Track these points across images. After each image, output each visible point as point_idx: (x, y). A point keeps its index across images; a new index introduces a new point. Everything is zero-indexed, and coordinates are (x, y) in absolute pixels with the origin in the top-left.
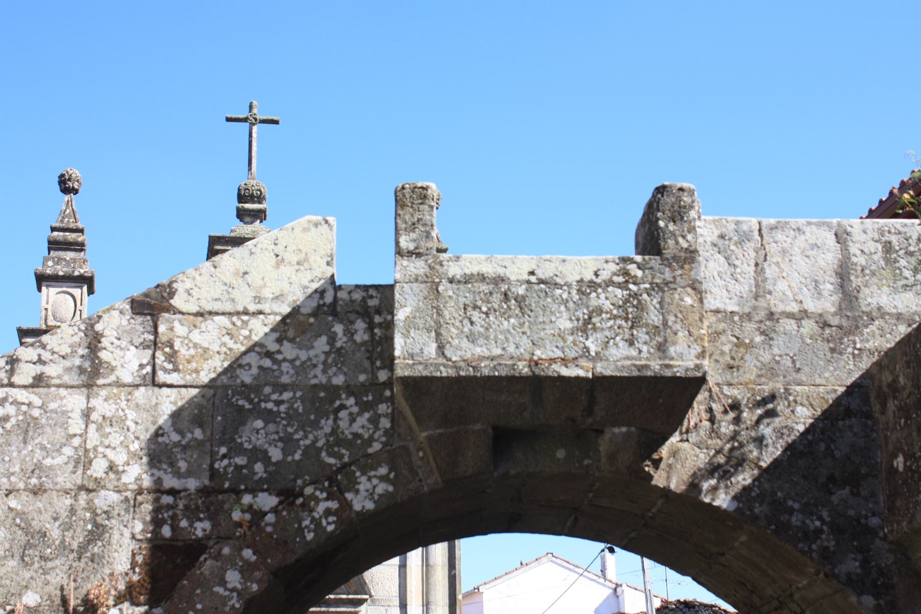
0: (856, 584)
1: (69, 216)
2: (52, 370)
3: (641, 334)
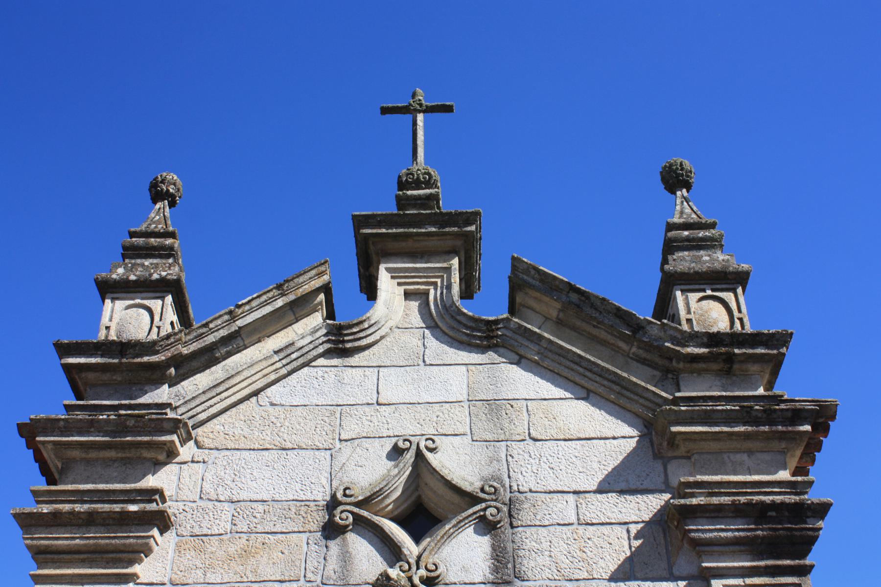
1: (159, 222)
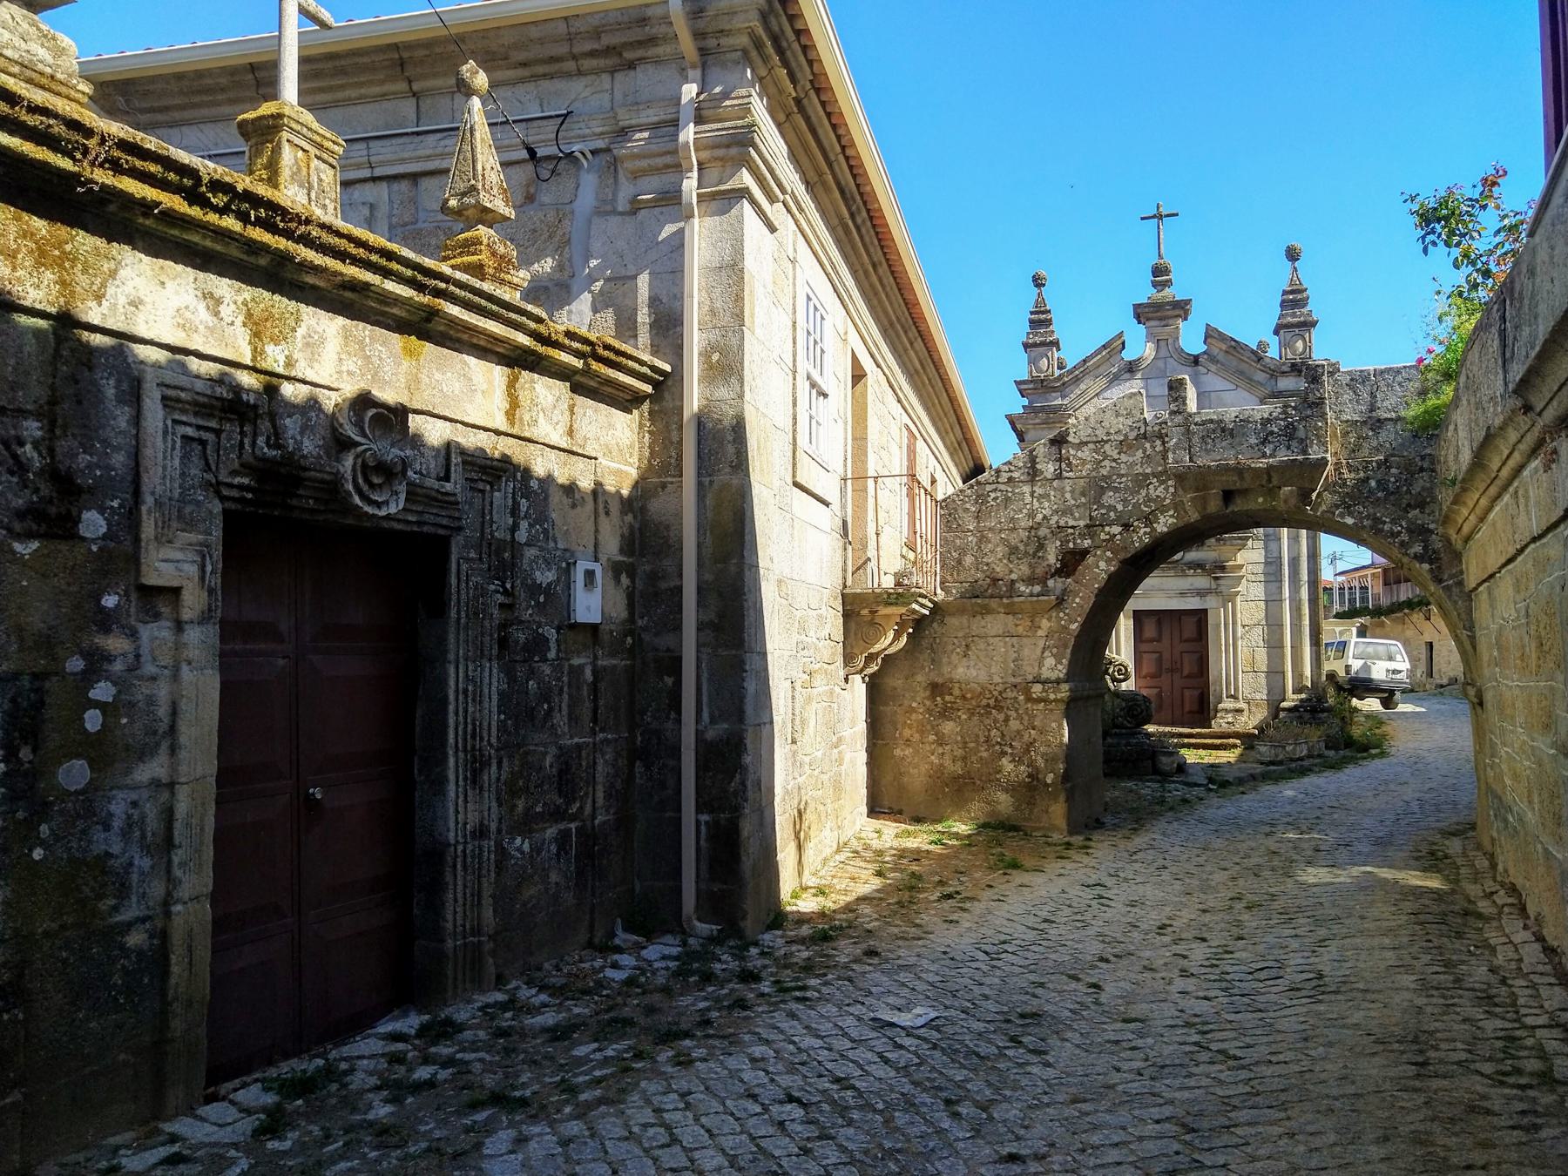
0: (1419, 558)
2: (1016, 475)
3: (1294, 443)
